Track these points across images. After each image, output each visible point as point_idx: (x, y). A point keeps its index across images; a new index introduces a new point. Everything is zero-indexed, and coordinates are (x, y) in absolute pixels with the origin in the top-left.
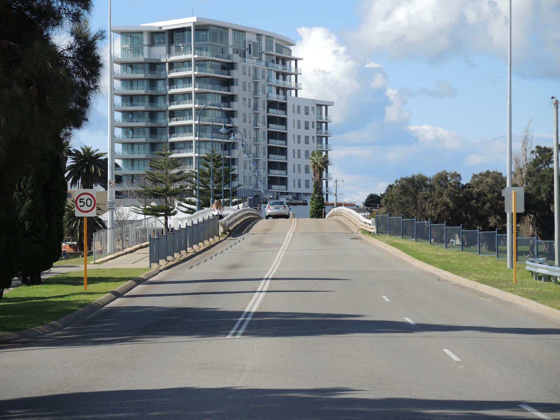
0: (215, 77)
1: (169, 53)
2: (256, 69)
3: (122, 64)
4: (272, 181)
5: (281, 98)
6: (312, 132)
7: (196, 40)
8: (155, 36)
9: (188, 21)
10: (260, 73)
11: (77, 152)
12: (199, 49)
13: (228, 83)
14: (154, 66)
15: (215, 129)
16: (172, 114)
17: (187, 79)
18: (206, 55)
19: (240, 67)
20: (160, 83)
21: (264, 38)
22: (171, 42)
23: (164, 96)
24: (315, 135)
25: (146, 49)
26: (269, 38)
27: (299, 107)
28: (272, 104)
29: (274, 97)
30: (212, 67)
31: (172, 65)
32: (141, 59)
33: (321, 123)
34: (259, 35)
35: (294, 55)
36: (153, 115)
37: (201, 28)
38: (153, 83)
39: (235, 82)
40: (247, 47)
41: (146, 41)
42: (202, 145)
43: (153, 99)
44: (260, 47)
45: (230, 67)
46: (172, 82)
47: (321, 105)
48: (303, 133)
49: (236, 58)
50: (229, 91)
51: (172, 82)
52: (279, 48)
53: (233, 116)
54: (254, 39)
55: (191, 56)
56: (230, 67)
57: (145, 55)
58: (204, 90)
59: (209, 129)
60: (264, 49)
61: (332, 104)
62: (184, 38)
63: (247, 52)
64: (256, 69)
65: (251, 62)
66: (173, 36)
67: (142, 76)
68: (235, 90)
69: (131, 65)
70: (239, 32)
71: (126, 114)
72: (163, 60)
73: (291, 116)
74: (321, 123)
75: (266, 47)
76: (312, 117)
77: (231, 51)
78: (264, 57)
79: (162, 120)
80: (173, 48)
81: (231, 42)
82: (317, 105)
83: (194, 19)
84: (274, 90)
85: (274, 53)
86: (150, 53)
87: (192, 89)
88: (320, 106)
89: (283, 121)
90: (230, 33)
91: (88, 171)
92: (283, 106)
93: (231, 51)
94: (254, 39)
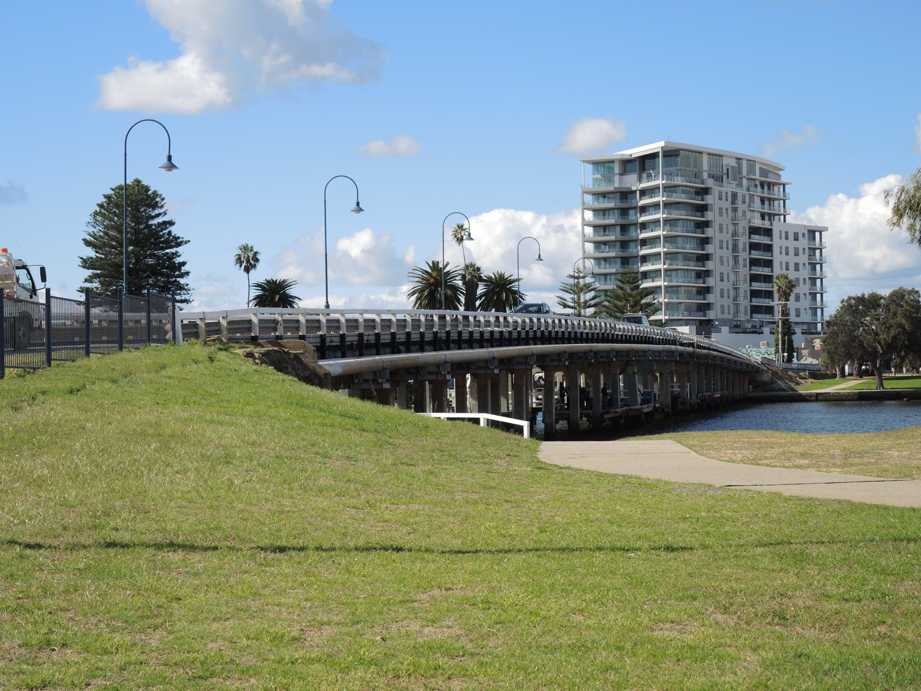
0: (686, 203)
1: (640, 180)
2: (734, 195)
3: (594, 194)
4: (755, 310)
5: (766, 224)
6: (804, 258)
7: (666, 165)
8: (627, 164)
9: (656, 146)
10: (740, 198)
11: (490, 278)
12: (668, 175)
13: (702, 209)
14: (626, 194)
15: (687, 257)
16: (644, 242)
17: (656, 206)
18: (679, 181)
20: (632, 212)
21: (744, 163)
22: (643, 169)
23: (636, 224)
24: (807, 262)
25: (617, 178)
26: (751, 163)
27: (787, 233)
28: (754, 231)
29: (757, 222)
30: (683, 192)
31: (643, 193)
32: (611, 189)
33: (815, 249)
35: (783, 180)
36: (624, 245)
37: (670, 154)
38: (624, 212)
39: (709, 207)
40: (725, 171)
41: (617, 170)
42: (674, 273)
43: (624, 228)
44: (740, 172)
45: (706, 191)
46: (644, 209)
47: (814, 232)
48: (792, 259)
49: (710, 183)
50: (703, 217)
51: (644, 209)
52: (764, 172)
53: (707, 243)
54: (733, 163)
55: (660, 182)
56: (706, 191)
57: (617, 183)
58: (673, 216)
59: (680, 257)
60: (744, 173)
61: (826, 229)
62: (654, 165)
63: (725, 177)
64: (734, 195)
65: (729, 187)
66: (644, 163)
67: (612, 205)
68: (709, 216)
69: (604, 195)
70: (716, 156)
71: (598, 244)
72: (634, 188)
73: (777, 243)
74: (815, 249)
75: (748, 173)
76: (803, 243)
77: (705, 175)
78: (745, 182)
79: (633, 250)
80: (644, 175)
81: (705, 167)
82: (809, 231)
83: (662, 144)
84: (758, 216)
85: (757, 176)
86: (621, 182)
87: (660, 215)
88: (812, 233)
89: (768, 248)
90: (705, 158)
91: (499, 298)
92: (768, 232)
93: (705, 175)
94: (733, 163)
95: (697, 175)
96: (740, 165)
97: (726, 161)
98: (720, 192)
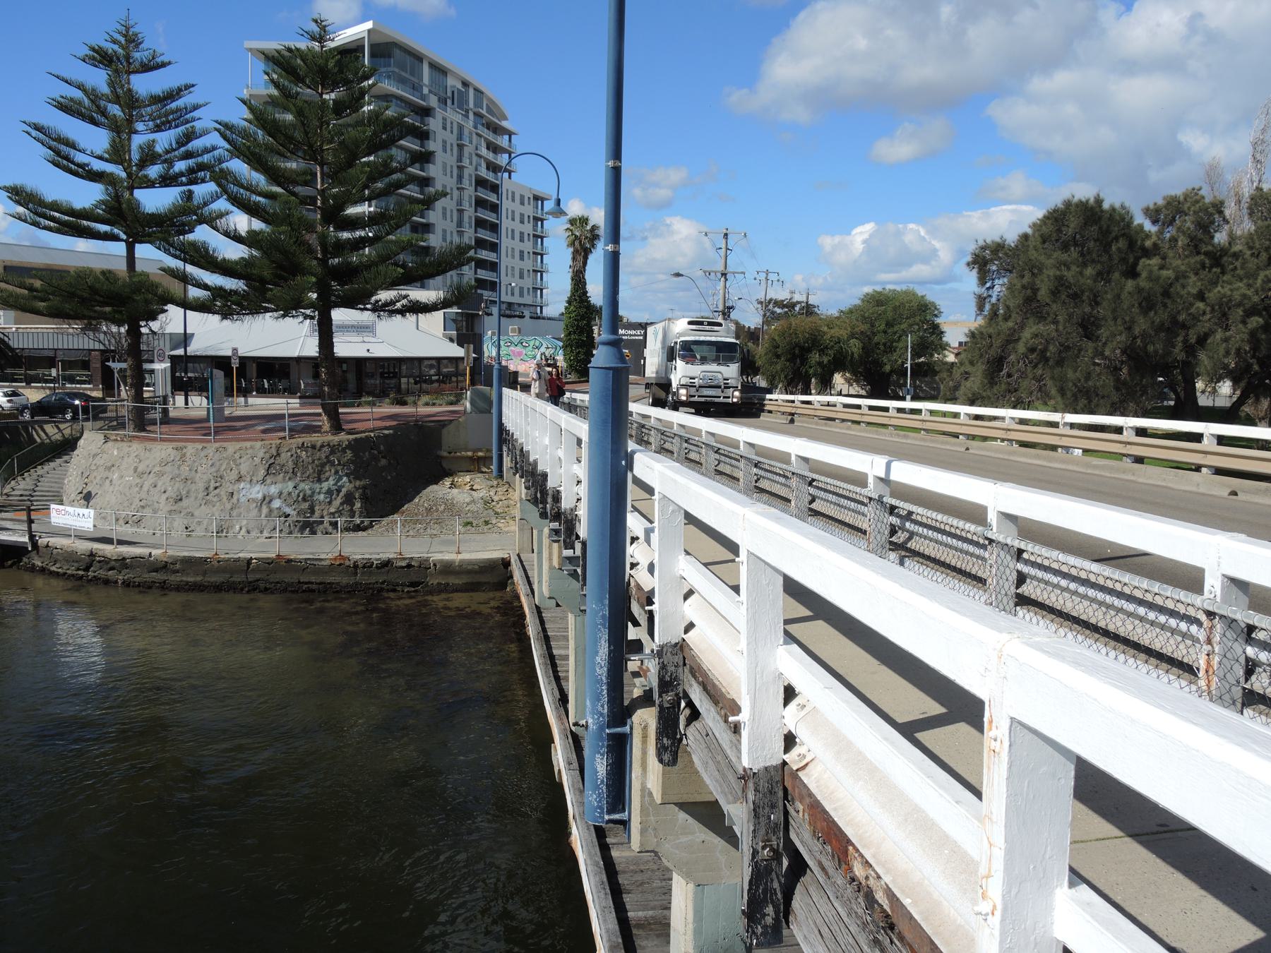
5: (490, 177)
10: (466, 132)
19: (439, 113)
21: (471, 92)
27: (513, 193)
28: (481, 183)
29: (483, 172)
34: (465, 84)
39: (431, 136)
40: (449, 94)
44: (467, 102)
45: (426, 112)
49: (433, 102)
56: (426, 112)
60: (471, 105)
63: (449, 102)
64: (461, 127)
70: (440, 71)
73: (506, 205)
75: (475, 105)
76: (528, 210)
77: (426, 91)
78: (471, 115)
81: (426, 80)
83: (369, 25)
84: (484, 165)
85: (484, 112)
88: (536, 198)
92: (495, 188)
95: (416, 88)
96: (467, 92)
97: (451, 82)
98: (444, 119)
